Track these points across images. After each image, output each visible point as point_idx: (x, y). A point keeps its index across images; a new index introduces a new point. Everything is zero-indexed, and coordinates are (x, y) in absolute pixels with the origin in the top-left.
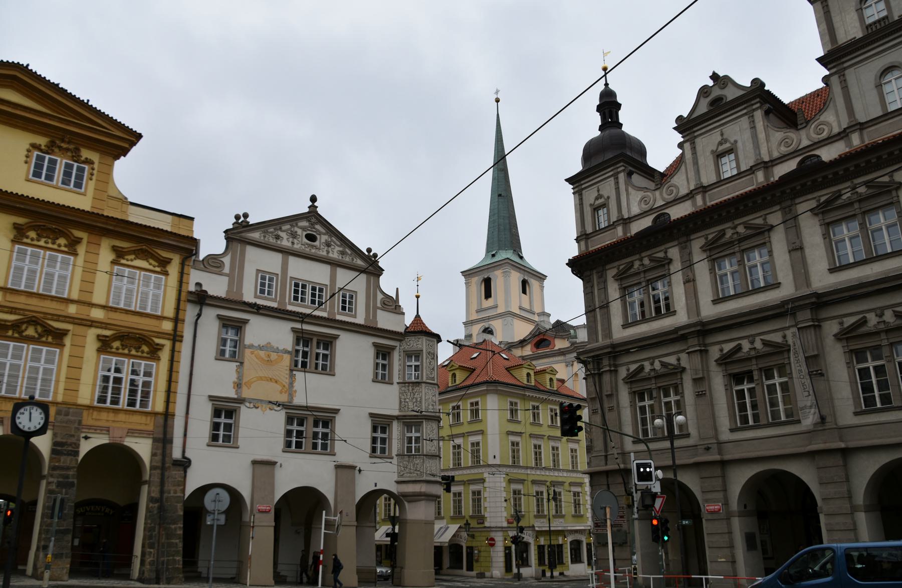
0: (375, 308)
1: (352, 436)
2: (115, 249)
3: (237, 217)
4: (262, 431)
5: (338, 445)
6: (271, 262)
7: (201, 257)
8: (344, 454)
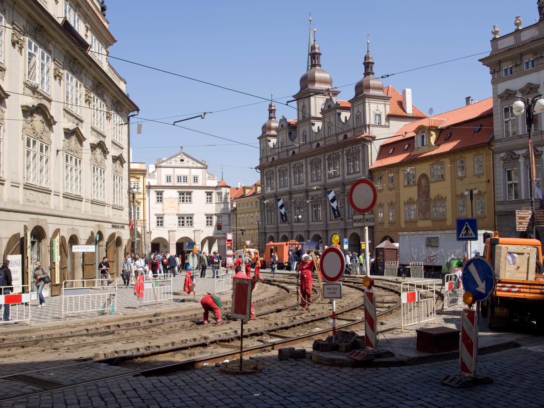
0: (206, 179)
1: (200, 221)
4: (171, 221)
5: (194, 225)
6: (169, 172)
8: (196, 226)
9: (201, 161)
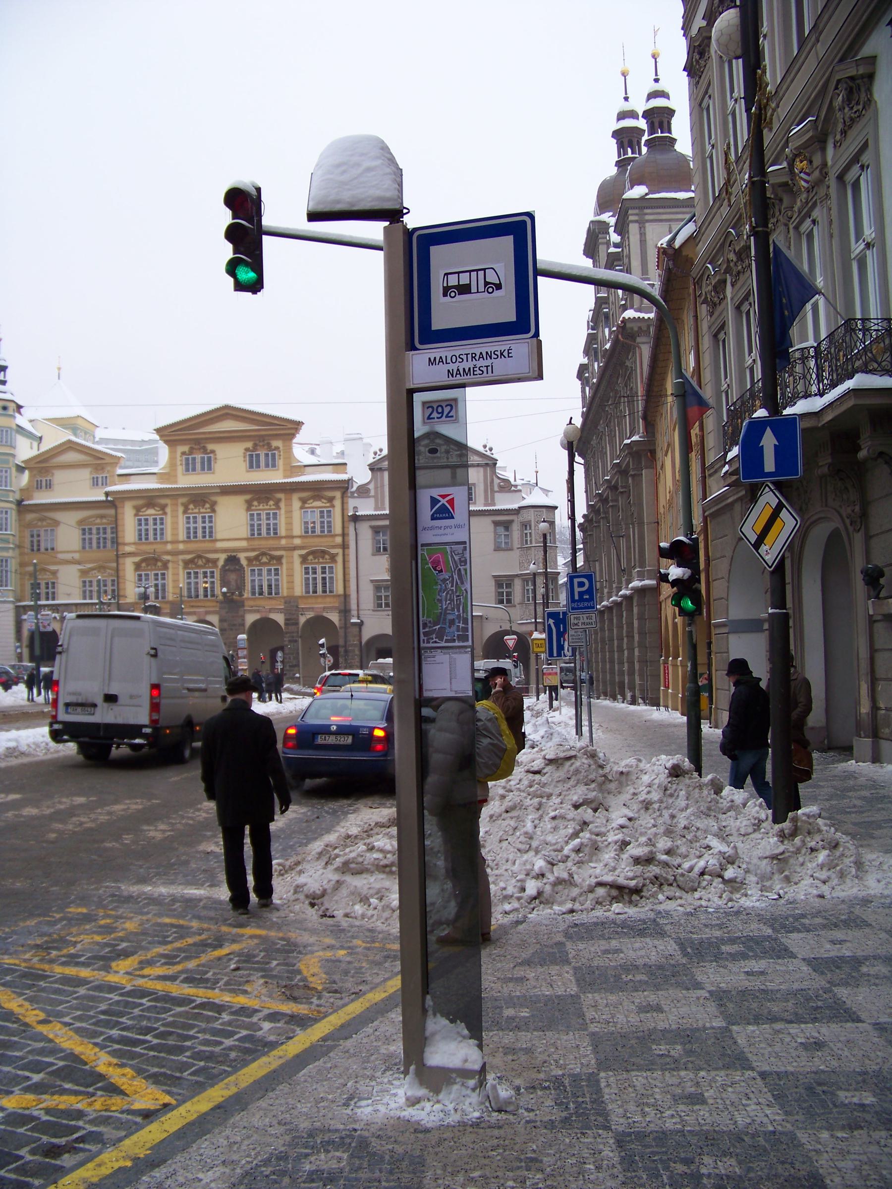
0: (493, 492)
2: (301, 499)
3: (375, 453)
7: (354, 489)
9: (481, 449)
